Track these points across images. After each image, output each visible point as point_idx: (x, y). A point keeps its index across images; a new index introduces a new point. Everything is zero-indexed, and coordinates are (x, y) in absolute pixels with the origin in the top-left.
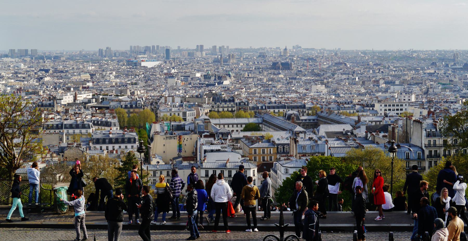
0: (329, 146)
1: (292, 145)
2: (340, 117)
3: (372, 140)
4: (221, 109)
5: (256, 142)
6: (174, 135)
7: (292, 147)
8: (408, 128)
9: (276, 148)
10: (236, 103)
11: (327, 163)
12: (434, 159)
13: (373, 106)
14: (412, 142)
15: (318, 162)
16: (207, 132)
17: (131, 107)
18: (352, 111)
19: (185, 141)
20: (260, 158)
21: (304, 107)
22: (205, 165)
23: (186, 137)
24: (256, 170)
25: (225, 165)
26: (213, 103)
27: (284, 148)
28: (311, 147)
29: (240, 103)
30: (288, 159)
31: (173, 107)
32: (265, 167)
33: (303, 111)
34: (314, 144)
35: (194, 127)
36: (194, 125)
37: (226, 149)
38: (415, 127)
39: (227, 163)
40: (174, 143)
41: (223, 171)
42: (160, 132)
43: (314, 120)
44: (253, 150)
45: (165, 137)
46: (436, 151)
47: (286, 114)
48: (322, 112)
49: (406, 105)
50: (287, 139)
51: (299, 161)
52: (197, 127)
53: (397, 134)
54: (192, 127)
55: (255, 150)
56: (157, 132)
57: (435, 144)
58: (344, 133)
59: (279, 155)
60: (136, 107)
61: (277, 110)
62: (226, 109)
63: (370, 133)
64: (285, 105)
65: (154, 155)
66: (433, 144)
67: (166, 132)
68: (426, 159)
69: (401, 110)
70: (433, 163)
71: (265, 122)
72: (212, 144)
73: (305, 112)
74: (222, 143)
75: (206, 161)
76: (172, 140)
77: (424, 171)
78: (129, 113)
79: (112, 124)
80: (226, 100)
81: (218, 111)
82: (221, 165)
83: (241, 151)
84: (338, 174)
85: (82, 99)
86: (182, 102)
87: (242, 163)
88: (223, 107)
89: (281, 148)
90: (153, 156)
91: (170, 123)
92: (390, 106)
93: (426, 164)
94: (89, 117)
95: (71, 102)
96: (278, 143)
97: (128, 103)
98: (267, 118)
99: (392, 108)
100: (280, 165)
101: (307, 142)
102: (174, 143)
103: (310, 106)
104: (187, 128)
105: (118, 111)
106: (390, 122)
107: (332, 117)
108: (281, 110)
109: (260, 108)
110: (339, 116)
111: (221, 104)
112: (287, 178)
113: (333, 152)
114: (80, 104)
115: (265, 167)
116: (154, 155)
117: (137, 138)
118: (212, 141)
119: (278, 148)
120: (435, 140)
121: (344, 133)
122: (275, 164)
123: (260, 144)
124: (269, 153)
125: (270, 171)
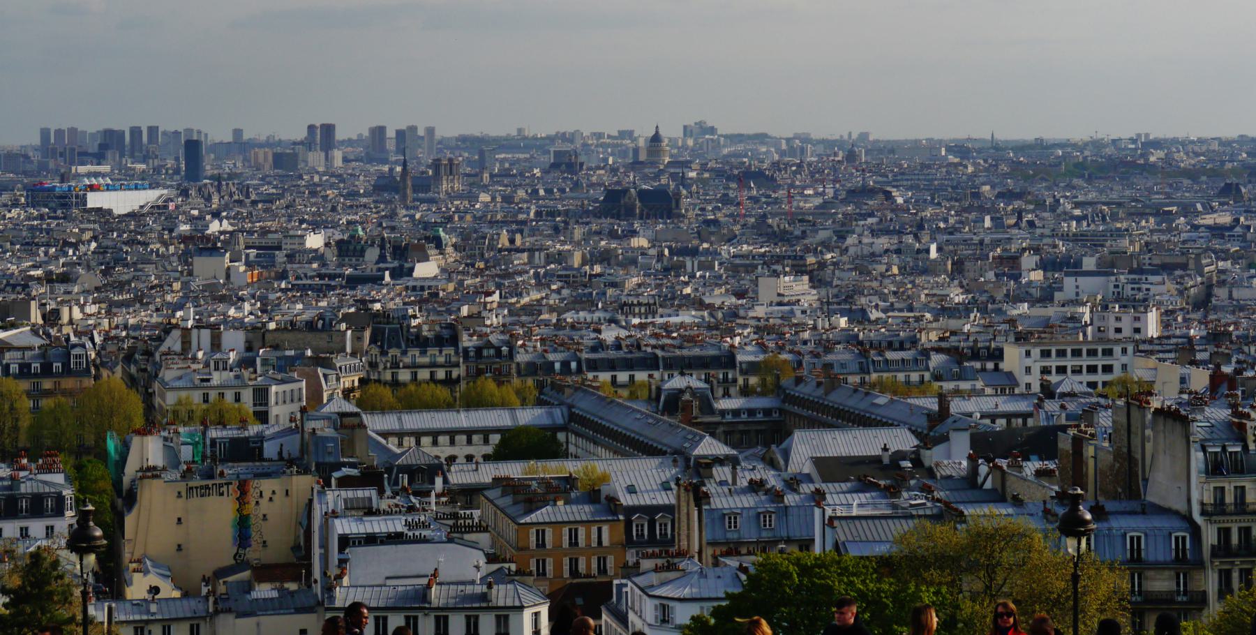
0: (829, 512)
1: (684, 510)
2: (868, 398)
3: (994, 490)
4: (405, 376)
6: (218, 481)
7: (684, 518)
8: (1136, 441)
9: (622, 526)
10: (466, 350)
11: (823, 578)
13: (998, 355)
14: (1152, 497)
15: (787, 575)
16: (352, 465)
17: (47, 370)
18: (915, 377)
19: (264, 502)
20: (558, 566)
21: (728, 360)
23: (267, 485)
24: (544, 611)
25: (422, 595)
26: (375, 351)
29: (479, 350)
30: (670, 567)
31: (217, 369)
32: (579, 601)
33: (726, 379)
35: (298, 447)
36: (298, 436)
37: (425, 533)
38: (1161, 435)
39: (429, 586)
41: (416, 618)
42: (164, 469)
43: (767, 412)
44: (533, 531)
45: (182, 487)
47: (659, 389)
48: (799, 380)
49: (1124, 351)
50: (665, 487)
51: (711, 572)
52: (312, 448)
53: (1091, 462)
54: (292, 445)
55: (541, 535)
56: (149, 469)
58: (886, 461)
59: (634, 551)
60: (67, 371)
61: (623, 377)
62: (424, 374)
63: (988, 460)
64: (656, 356)
65: (139, 561)
66: (1236, 504)
67: (189, 470)
68: (1208, 564)
69: (1108, 369)
70: (1235, 575)
71: (578, 422)
72: (370, 512)
73: (735, 381)
74: (411, 509)
75: (346, 581)
76: (213, 501)
77: (1200, 610)
78: (36, 394)
80: (427, 339)
81: (395, 384)
82: (405, 596)
83: (484, 538)
84: (868, 623)
86: (249, 348)
87: (490, 586)
88: (414, 366)
89: (640, 522)
90: (134, 565)
91: (204, 434)
92: (1062, 353)
93: (1211, 583)
96: (630, 503)
97: (35, 357)
98: (584, 405)
99: (1069, 362)
100: (637, 591)
101: (744, 498)
103: (751, 358)
104: (270, 450)
106: (1064, 415)
107: (837, 398)
108: (641, 376)
109: (557, 366)
110: (867, 394)
111: (404, 353)
113: (843, 538)
116: (139, 561)
117: (68, 493)
118: (370, 499)
119: (628, 524)
120: (1243, 488)
121: (886, 461)
122: (620, 586)
123: (560, 511)
124: (594, 544)
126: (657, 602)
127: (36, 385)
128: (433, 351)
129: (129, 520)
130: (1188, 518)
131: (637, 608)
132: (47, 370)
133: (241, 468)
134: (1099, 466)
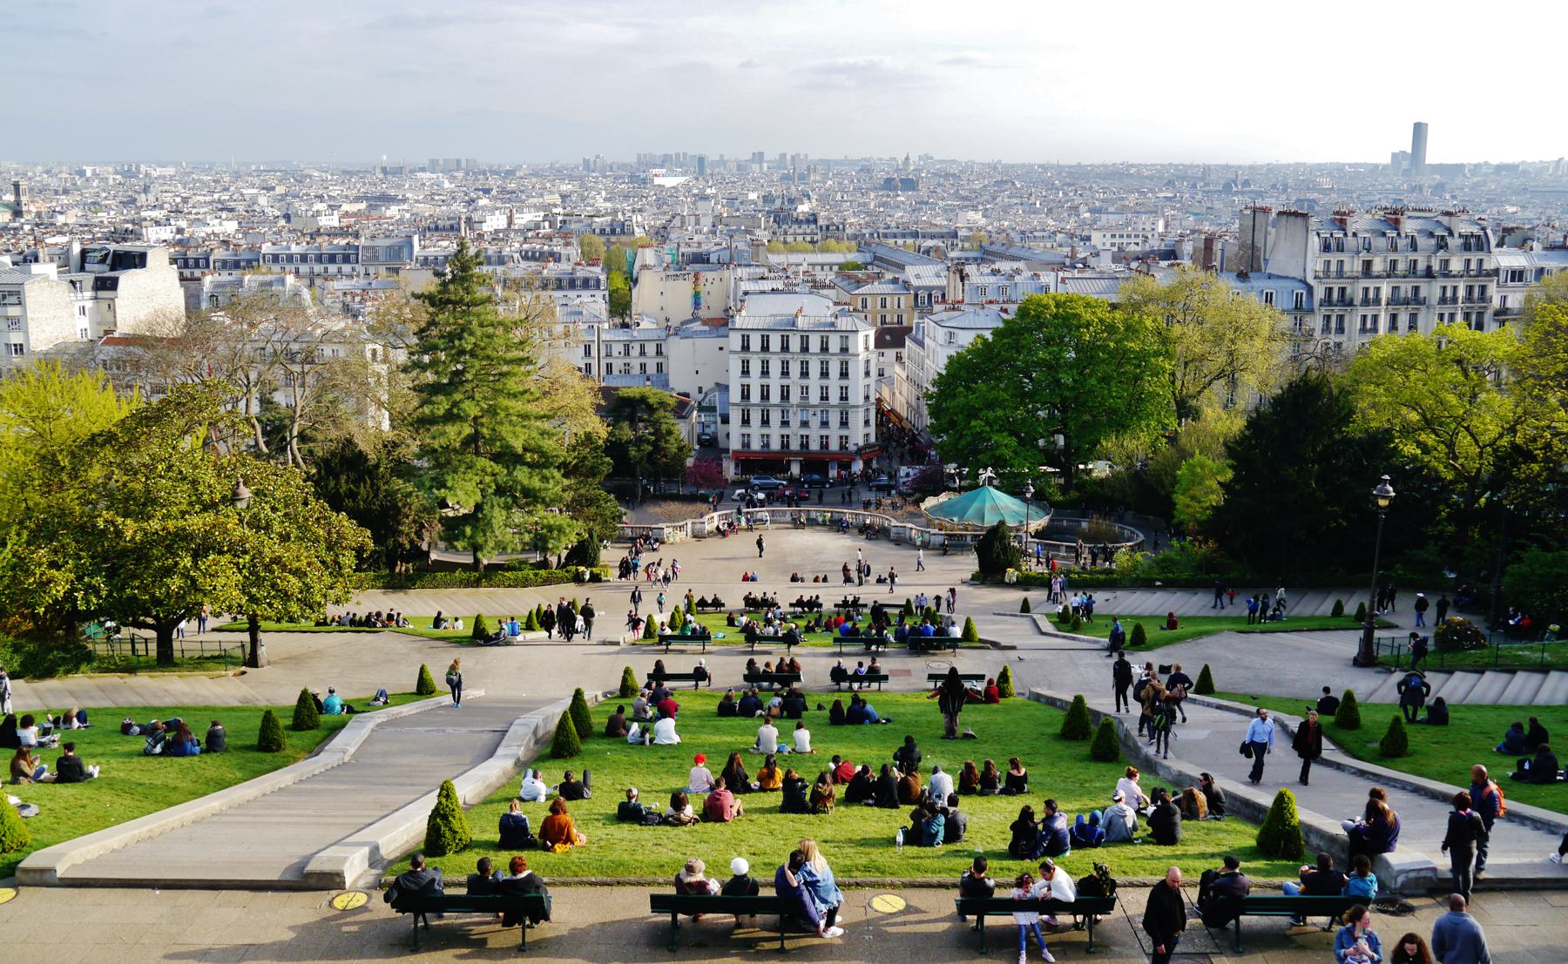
1: (952, 285)
4: (790, 239)
8: (1259, 236)
12: (1337, 310)
13: (1088, 238)
14: (1272, 269)
15: (1046, 307)
17: (613, 232)
18: (1049, 245)
19: (708, 284)
20: (875, 319)
22: (739, 322)
23: (710, 275)
24: (872, 333)
25: (794, 324)
26: (776, 226)
27: (930, 296)
28: (1002, 289)
29: (828, 227)
32: (888, 338)
34: (1007, 283)
37: (797, 289)
39: (797, 316)
40: (684, 288)
44: (860, 299)
46: (1343, 290)
48: (992, 243)
50: (938, 275)
51: (981, 312)
53: (1219, 253)
54: (725, 256)
57: (1341, 271)
60: (623, 232)
61: (900, 242)
62: (800, 238)
70: (1334, 319)
72: (762, 278)
75: (744, 313)
76: (681, 282)
81: (785, 242)
83: (832, 293)
85: (524, 222)
88: (795, 234)
92: (1122, 236)
93: (1315, 322)
94: (517, 245)
95: (501, 227)
98: (881, 252)
99: (1125, 240)
102: (684, 288)
104: (713, 258)
105: (586, 241)
107: (1012, 251)
108: (910, 241)
112: (950, 358)
114: (519, 230)
115: (888, 338)
117: (603, 277)
119: (916, 296)
121: (1068, 263)
122: (918, 324)
127: (608, 240)
128: (804, 226)
130: (1304, 282)
132: (613, 232)
133: (697, 267)
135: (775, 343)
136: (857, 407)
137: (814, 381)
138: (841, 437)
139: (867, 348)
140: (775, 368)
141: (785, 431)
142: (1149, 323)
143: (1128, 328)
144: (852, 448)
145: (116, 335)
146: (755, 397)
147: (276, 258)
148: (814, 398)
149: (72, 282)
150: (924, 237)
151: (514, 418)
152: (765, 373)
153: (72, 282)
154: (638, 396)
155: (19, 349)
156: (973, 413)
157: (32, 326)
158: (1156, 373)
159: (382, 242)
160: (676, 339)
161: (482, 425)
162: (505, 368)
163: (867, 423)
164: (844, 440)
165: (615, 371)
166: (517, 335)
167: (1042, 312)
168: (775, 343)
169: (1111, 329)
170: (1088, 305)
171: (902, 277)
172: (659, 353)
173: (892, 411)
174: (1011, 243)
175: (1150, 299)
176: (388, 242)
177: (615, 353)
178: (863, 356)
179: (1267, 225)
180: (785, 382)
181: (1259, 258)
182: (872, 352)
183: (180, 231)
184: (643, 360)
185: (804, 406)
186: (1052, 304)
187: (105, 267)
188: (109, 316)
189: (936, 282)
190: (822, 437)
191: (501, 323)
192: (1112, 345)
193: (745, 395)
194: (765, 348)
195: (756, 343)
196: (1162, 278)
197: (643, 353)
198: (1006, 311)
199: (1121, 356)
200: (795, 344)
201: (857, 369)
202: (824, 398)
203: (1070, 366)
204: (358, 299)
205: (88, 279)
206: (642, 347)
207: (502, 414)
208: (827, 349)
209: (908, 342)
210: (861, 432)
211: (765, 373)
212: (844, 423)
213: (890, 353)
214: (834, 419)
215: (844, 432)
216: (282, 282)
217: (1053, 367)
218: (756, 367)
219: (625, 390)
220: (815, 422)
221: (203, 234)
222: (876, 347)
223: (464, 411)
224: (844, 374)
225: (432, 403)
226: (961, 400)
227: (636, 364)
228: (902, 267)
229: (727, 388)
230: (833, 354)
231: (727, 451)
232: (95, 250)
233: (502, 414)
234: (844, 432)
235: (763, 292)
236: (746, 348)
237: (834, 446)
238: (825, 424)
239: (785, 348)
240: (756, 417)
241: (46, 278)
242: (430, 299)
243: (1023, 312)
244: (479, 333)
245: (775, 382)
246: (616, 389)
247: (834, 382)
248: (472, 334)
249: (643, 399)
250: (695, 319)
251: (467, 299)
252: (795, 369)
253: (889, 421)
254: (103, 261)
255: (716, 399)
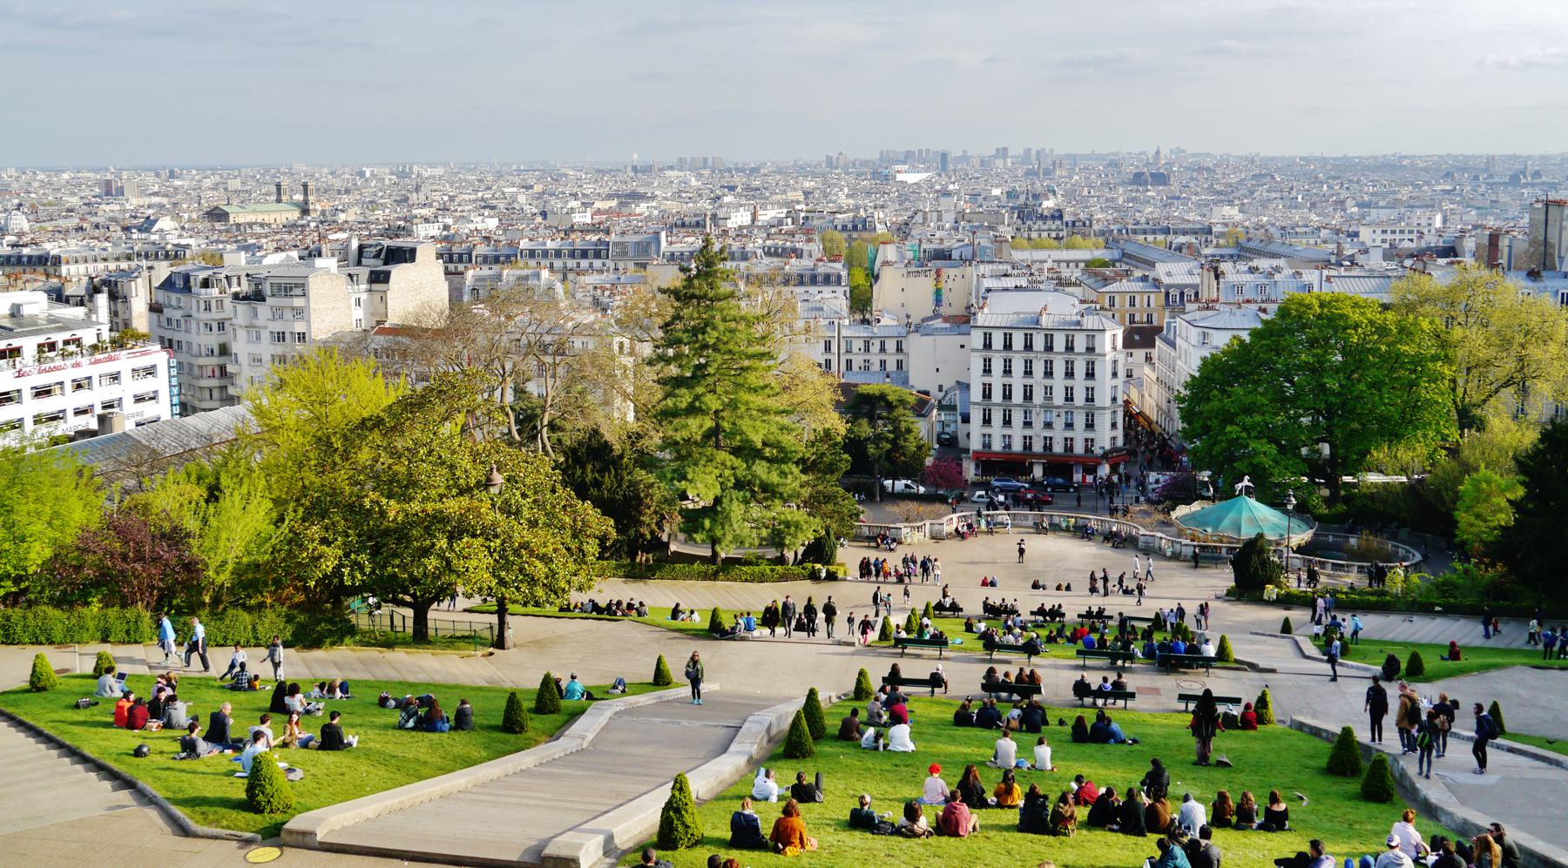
4: (1034, 235)
5: (1115, 281)
9: (1163, 296)
10: (1067, 223)
13: (1356, 234)
15: (1309, 307)
17: (855, 228)
18: (1312, 241)
19: (950, 281)
20: (1123, 318)
22: (981, 319)
23: (952, 272)
25: (1037, 322)
26: (1020, 222)
27: (1182, 294)
28: (1261, 288)
29: (1074, 223)
30: (1208, 308)
32: (1137, 337)
34: (1266, 281)
37: (1042, 286)
39: (1041, 314)
40: (923, 287)
48: (1249, 240)
50: (1191, 273)
51: (1238, 312)
53: (1506, 251)
54: (968, 253)
55: (1112, 300)
61: (1150, 238)
62: (1044, 235)
72: (1006, 275)
75: (986, 310)
76: (922, 278)
78: (850, 239)
79: (805, 254)
81: (1029, 239)
82: (1024, 321)
83: (1077, 290)
87: (1082, 316)
88: (1040, 230)
92: (1393, 232)
98: (1130, 249)
99: (1398, 236)
102: (923, 287)
104: (955, 255)
107: (1271, 248)
108: (1160, 237)
112: (1204, 359)
114: (760, 228)
117: (844, 273)
119: (1167, 294)
121: (1333, 261)
122: (1169, 324)
123: (1124, 285)
125: (1153, 345)
126: (1200, 330)
128: (1049, 222)
129: (875, 288)
131: (1183, 335)
132: (855, 228)
134: (1514, 251)
135: (1018, 341)
136: (1104, 408)
137: (1059, 382)
138: (1087, 440)
139: (1114, 348)
140: (1018, 367)
141: (1028, 432)
142: (1425, 325)
143: (1402, 330)
144: (1098, 451)
145: (387, 325)
146: (997, 396)
147: (532, 254)
148: (1059, 398)
149: (350, 275)
150: (1175, 233)
151: (754, 413)
152: (1008, 372)
153: (350, 275)
154: (877, 393)
155: (302, 337)
156: (1228, 418)
157: (314, 317)
158: (1435, 378)
159: (631, 238)
160: (918, 335)
161: (723, 418)
162: (746, 363)
163: (1114, 425)
164: (1089, 443)
165: (855, 367)
166: (759, 330)
167: (1304, 312)
168: (1018, 341)
169: (1382, 331)
170: (1356, 305)
171: (1151, 274)
172: (899, 349)
173: (1141, 414)
174: (1270, 240)
175: (1426, 299)
176: (637, 238)
177: (855, 350)
178: (1109, 357)
179: (1562, 220)
180: (1028, 381)
181: (1552, 255)
182: (1120, 352)
183: (446, 227)
184: (883, 357)
185: (1048, 406)
186: (1316, 303)
187: (380, 262)
188: (381, 308)
189: (1188, 280)
190: (1066, 439)
191: (743, 318)
192: (1383, 348)
193: (987, 394)
194: (1008, 346)
195: (998, 341)
196: (1440, 276)
197: (883, 350)
198: (1264, 311)
199: (1394, 360)
200: (1039, 342)
201: (1103, 369)
202: (1069, 398)
203: (1336, 370)
204: (607, 293)
205: (364, 273)
206: (883, 344)
207: (743, 408)
208: (1072, 348)
209: (1158, 342)
210: (1107, 435)
211: (1008, 372)
212: (1090, 426)
213: (1140, 354)
214: (1079, 420)
215: (1090, 435)
216: (538, 276)
217: (1317, 370)
218: (997, 366)
219: (864, 387)
220: (1059, 424)
221: (467, 231)
222: (1125, 346)
223: (706, 404)
224: (1090, 375)
225: (675, 396)
226: (1215, 404)
227: (875, 360)
228: (1152, 265)
229: (968, 386)
230: (1078, 354)
231: (967, 451)
232: (371, 246)
233: (743, 408)
234: (1090, 435)
235: (1006, 290)
236: (988, 346)
237: (1079, 449)
238: (1069, 426)
239: (1028, 347)
240: (997, 417)
241: (327, 271)
242: (675, 293)
243: (1284, 312)
244: (722, 327)
245: (1018, 382)
246: (856, 385)
247: (1079, 383)
248: (714, 328)
249: (883, 397)
250: (936, 316)
251: (711, 294)
252: (1038, 369)
253: (1138, 424)
254: (377, 256)
255: (957, 397)
